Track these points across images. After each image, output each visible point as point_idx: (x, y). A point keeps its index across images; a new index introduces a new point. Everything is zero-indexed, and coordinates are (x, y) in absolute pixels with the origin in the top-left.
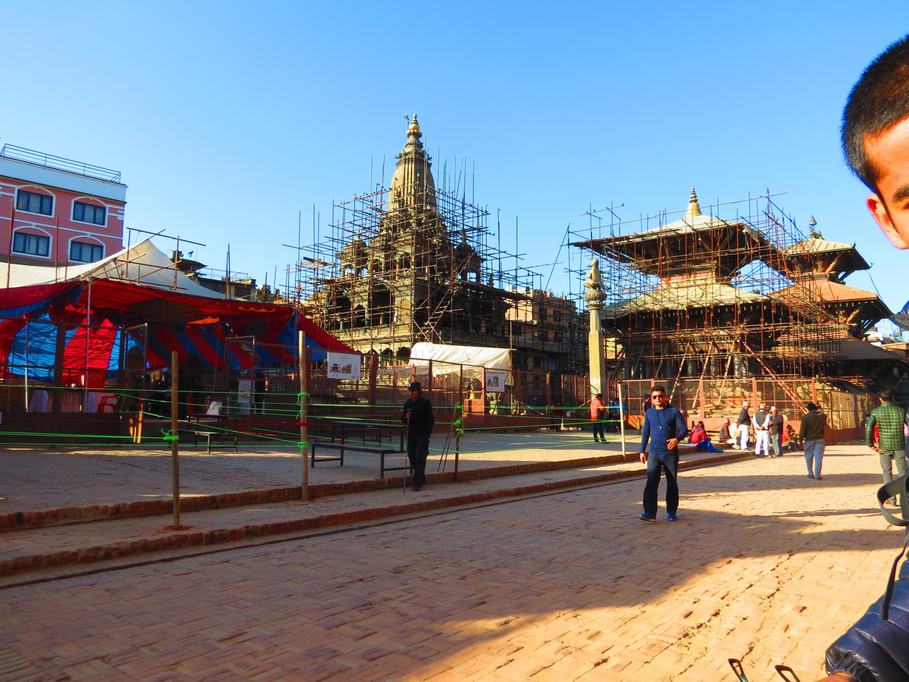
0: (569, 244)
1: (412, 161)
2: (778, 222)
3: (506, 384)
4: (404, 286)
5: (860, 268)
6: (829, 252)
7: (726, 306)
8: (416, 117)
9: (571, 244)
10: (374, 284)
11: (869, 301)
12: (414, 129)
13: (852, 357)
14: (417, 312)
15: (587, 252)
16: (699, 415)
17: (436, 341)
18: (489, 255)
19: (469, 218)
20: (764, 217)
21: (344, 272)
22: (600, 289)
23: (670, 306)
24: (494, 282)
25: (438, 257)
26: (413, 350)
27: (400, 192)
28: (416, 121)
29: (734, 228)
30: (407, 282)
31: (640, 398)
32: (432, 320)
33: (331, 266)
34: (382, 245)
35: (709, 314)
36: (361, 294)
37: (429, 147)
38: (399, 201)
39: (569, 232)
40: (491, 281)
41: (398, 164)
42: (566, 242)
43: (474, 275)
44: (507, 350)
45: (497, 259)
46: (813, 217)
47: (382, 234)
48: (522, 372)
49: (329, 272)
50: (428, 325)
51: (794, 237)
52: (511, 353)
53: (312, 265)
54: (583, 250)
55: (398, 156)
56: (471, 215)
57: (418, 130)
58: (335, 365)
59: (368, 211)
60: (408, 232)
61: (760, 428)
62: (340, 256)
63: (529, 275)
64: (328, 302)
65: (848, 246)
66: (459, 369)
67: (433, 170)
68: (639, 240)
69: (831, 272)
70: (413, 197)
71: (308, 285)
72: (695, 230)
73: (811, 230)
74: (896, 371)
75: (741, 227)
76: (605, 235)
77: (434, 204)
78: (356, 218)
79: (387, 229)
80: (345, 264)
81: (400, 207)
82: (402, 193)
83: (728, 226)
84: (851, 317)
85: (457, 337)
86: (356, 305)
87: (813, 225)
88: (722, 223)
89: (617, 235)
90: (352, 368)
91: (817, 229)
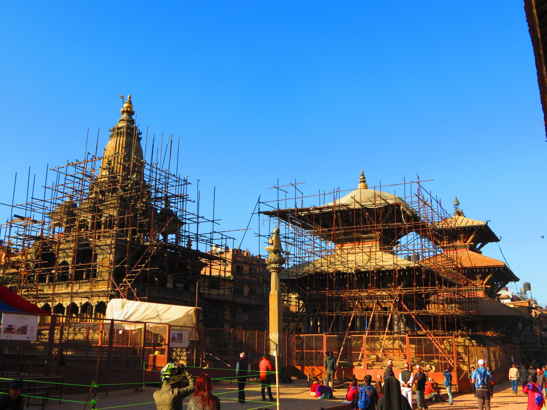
0: (259, 213)
1: (123, 134)
2: (427, 203)
3: (190, 339)
4: (106, 245)
5: (492, 241)
6: (469, 227)
8: (130, 98)
9: (261, 212)
10: (79, 241)
11: (499, 267)
12: (128, 107)
14: (116, 270)
15: (274, 220)
16: (362, 367)
17: (130, 297)
18: (189, 219)
19: (173, 186)
20: (416, 199)
22: (280, 254)
23: (341, 268)
24: (193, 243)
25: (140, 220)
26: (109, 305)
27: (111, 160)
28: (131, 101)
29: (392, 205)
30: (109, 242)
31: (314, 351)
32: (128, 278)
33: (41, 224)
34: (90, 206)
37: (140, 124)
38: (110, 168)
39: (260, 202)
40: (189, 244)
41: (111, 136)
42: (257, 211)
43: (174, 236)
45: (195, 222)
47: (91, 197)
48: (205, 328)
49: (39, 229)
50: (125, 282)
51: (440, 215)
52: (197, 312)
53: (22, 222)
54: (272, 218)
55: (112, 129)
56: (174, 184)
57: (131, 108)
59: (81, 176)
60: (114, 197)
61: (406, 385)
62: (52, 214)
63: (222, 238)
64: (35, 256)
65: (482, 223)
66: (143, 326)
67: (142, 143)
68: (318, 212)
69: (471, 243)
70: (121, 166)
71: (18, 240)
72: (363, 206)
73: (455, 208)
74: (520, 325)
75: (398, 205)
77: (141, 174)
78: (67, 182)
79: (96, 193)
80: (55, 222)
82: (113, 162)
84: (487, 280)
85: (154, 292)
86: (61, 261)
87: (456, 205)
88: (383, 201)
89: (299, 207)
90: (29, 328)
91: (460, 208)
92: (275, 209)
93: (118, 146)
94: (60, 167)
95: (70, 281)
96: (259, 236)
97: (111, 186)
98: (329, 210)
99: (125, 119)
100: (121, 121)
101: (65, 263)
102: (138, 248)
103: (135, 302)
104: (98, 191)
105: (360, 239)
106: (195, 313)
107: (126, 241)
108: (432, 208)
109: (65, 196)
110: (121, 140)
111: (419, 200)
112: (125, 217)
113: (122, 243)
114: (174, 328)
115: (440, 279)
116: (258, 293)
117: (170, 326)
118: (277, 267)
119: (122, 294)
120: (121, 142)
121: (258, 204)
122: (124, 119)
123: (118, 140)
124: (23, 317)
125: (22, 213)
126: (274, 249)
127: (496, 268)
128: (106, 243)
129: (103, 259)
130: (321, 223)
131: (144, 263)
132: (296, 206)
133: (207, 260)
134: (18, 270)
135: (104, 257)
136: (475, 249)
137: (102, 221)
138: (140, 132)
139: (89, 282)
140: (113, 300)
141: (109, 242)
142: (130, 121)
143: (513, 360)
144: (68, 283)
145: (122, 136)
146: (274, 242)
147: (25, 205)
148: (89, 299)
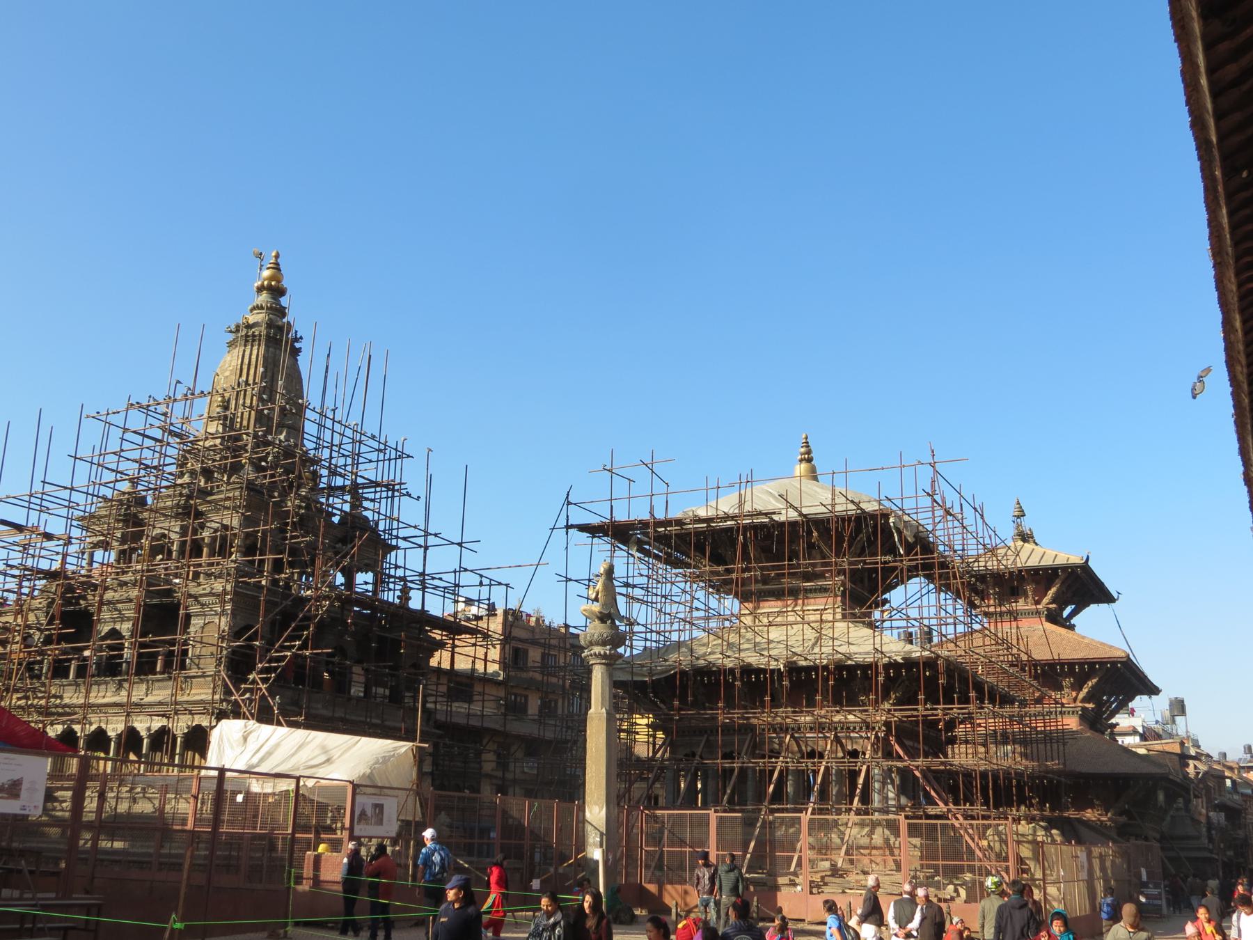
0: (568, 527)
1: (260, 340)
3: (401, 818)
4: (212, 594)
5: (1098, 601)
7: (858, 666)
8: (277, 257)
9: (572, 526)
12: (271, 278)
13: (1084, 769)
14: (234, 652)
15: (603, 545)
16: (799, 888)
17: (265, 716)
18: (405, 539)
19: (370, 461)
20: (927, 501)
21: (92, 556)
22: (613, 622)
23: (753, 659)
24: (412, 593)
25: (293, 537)
26: (215, 736)
27: (229, 399)
28: (277, 264)
29: (873, 516)
30: (218, 586)
31: (688, 849)
32: (261, 672)
33: (61, 542)
34: (178, 504)
35: (826, 680)
36: (120, 606)
37: (299, 316)
38: (225, 418)
39: (569, 503)
41: (232, 344)
42: (562, 523)
43: (369, 577)
44: (404, 747)
45: (420, 546)
46: (1018, 503)
47: (179, 481)
49: (58, 553)
50: (254, 682)
51: (981, 540)
53: (19, 538)
54: (596, 540)
55: (233, 328)
56: (373, 456)
57: (279, 281)
59: (158, 434)
60: (234, 483)
62: (88, 521)
63: (481, 584)
64: (46, 617)
65: (1076, 559)
67: (303, 360)
69: (1051, 606)
70: (253, 413)
71: (8, 579)
72: (805, 516)
73: (1015, 525)
74: (1161, 797)
75: (886, 516)
76: (640, 513)
77: (296, 431)
78: (126, 446)
79: (193, 473)
80: (95, 539)
81: (224, 431)
83: (863, 511)
84: (1085, 690)
85: (320, 706)
86: (106, 629)
87: (1018, 517)
88: (851, 506)
89: (660, 515)
90: (25, 786)
91: (1027, 524)
92: (604, 520)
93: (245, 368)
94: (110, 412)
95: (126, 677)
96: (567, 581)
97: (227, 458)
98: (729, 523)
101: (114, 634)
102: (285, 603)
104: (198, 470)
105: (797, 591)
106: (415, 757)
107: (258, 586)
108: (962, 524)
109: (119, 479)
110: (255, 352)
111: (933, 504)
112: (258, 531)
113: (248, 590)
115: (979, 686)
116: (560, 711)
118: (605, 653)
119: (245, 709)
120: (254, 357)
121: (565, 506)
122: (262, 305)
123: (247, 353)
124: (13, 759)
125: (18, 516)
126: (600, 613)
127: (1107, 662)
128: (212, 589)
129: (203, 628)
131: (299, 638)
132: (651, 513)
133: (444, 633)
134: (5, 648)
135: (207, 621)
136: (1059, 618)
137: (203, 539)
138: (298, 336)
139: (170, 678)
140: (225, 723)
141: (218, 586)
142: (276, 309)
143: (1144, 878)
144: (120, 681)
145: (257, 343)
146: (599, 596)
147: (27, 498)
148: (168, 718)
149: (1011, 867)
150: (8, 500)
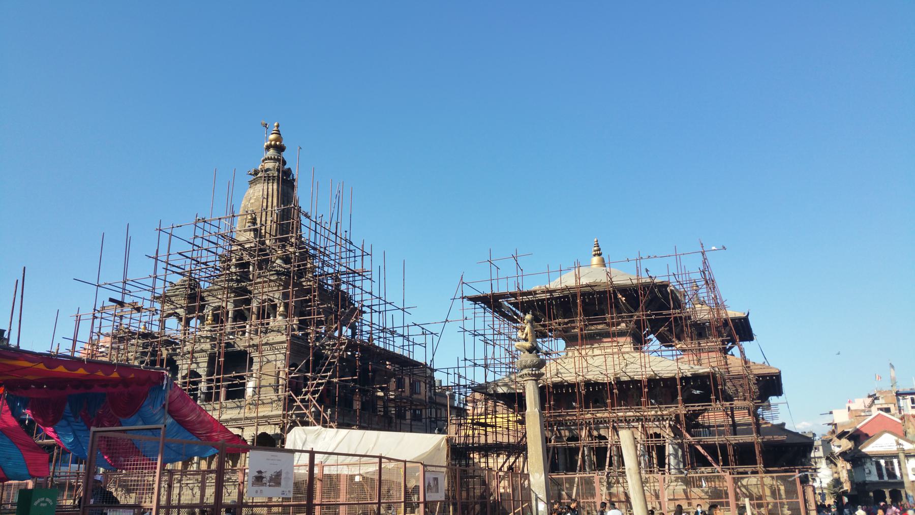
7: (662, 379)
8: (278, 126)
12: (276, 140)
17: (325, 424)
28: (278, 131)
54: (477, 306)
57: (281, 142)
58: (260, 472)
62: (165, 299)
81: (255, 238)
90: (283, 476)
99: (273, 157)
100: (266, 159)
103: (337, 431)
106: (448, 445)
110: (270, 187)
114: (429, 468)
117: (425, 466)
120: (270, 190)
121: (461, 285)
123: (265, 188)
124: (276, 456)
127: (768, 376)
130: (553, 312)
147: (121, 285)
149: (800, 502)
150: (106, 286)
